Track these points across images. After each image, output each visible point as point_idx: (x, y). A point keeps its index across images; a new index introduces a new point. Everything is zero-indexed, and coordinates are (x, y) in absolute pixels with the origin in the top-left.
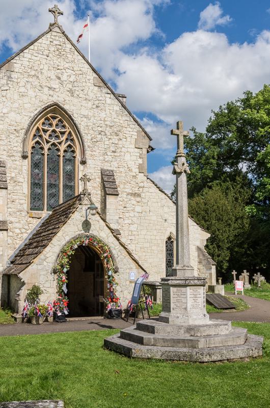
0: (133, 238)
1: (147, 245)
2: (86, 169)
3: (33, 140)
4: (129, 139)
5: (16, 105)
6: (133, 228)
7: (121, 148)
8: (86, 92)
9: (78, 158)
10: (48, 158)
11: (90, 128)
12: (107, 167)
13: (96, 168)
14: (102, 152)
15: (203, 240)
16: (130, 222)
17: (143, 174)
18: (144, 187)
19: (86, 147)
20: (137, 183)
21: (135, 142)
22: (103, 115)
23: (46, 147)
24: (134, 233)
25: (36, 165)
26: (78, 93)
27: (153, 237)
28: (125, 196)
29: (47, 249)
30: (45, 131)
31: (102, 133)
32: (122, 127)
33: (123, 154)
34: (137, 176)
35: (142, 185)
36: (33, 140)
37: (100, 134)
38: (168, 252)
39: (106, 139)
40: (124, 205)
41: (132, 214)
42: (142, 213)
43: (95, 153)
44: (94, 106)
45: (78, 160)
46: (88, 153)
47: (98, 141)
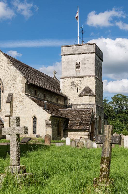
1: (24, 120)
8: (4, 67)
11: (5, 79)
12: (11, 92)
15: (48, 117)
22: (10, 74)
31: (10, 80)
32: (16, 77)
35: (23, 97)
38: (34, 122)
42: (23, 108)
43: (7, 88)
44: (7, 71)
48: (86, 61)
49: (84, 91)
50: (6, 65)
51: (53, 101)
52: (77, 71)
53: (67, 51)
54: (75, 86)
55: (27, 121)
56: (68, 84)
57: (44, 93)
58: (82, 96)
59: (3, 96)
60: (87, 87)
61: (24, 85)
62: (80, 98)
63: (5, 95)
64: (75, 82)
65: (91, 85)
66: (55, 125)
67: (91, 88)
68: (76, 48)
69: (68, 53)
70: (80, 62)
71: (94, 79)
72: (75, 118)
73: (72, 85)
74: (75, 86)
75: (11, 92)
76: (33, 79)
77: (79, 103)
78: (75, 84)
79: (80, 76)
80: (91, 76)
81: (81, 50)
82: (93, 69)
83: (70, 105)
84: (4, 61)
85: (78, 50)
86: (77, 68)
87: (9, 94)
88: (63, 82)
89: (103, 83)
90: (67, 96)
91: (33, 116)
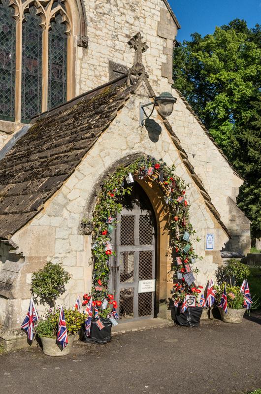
4: (148, 20)
9: (74, 37)
10: (23, 28)
13: (102, 60)
14: (110, 33)
17: (166, 80)
19: (88, 19)
21: (158, 27)
29: (71, 182)
34: (159, 82)
45: (74, 39)
46: (90, 29)
63: (95, 62)
75: (120, 56)
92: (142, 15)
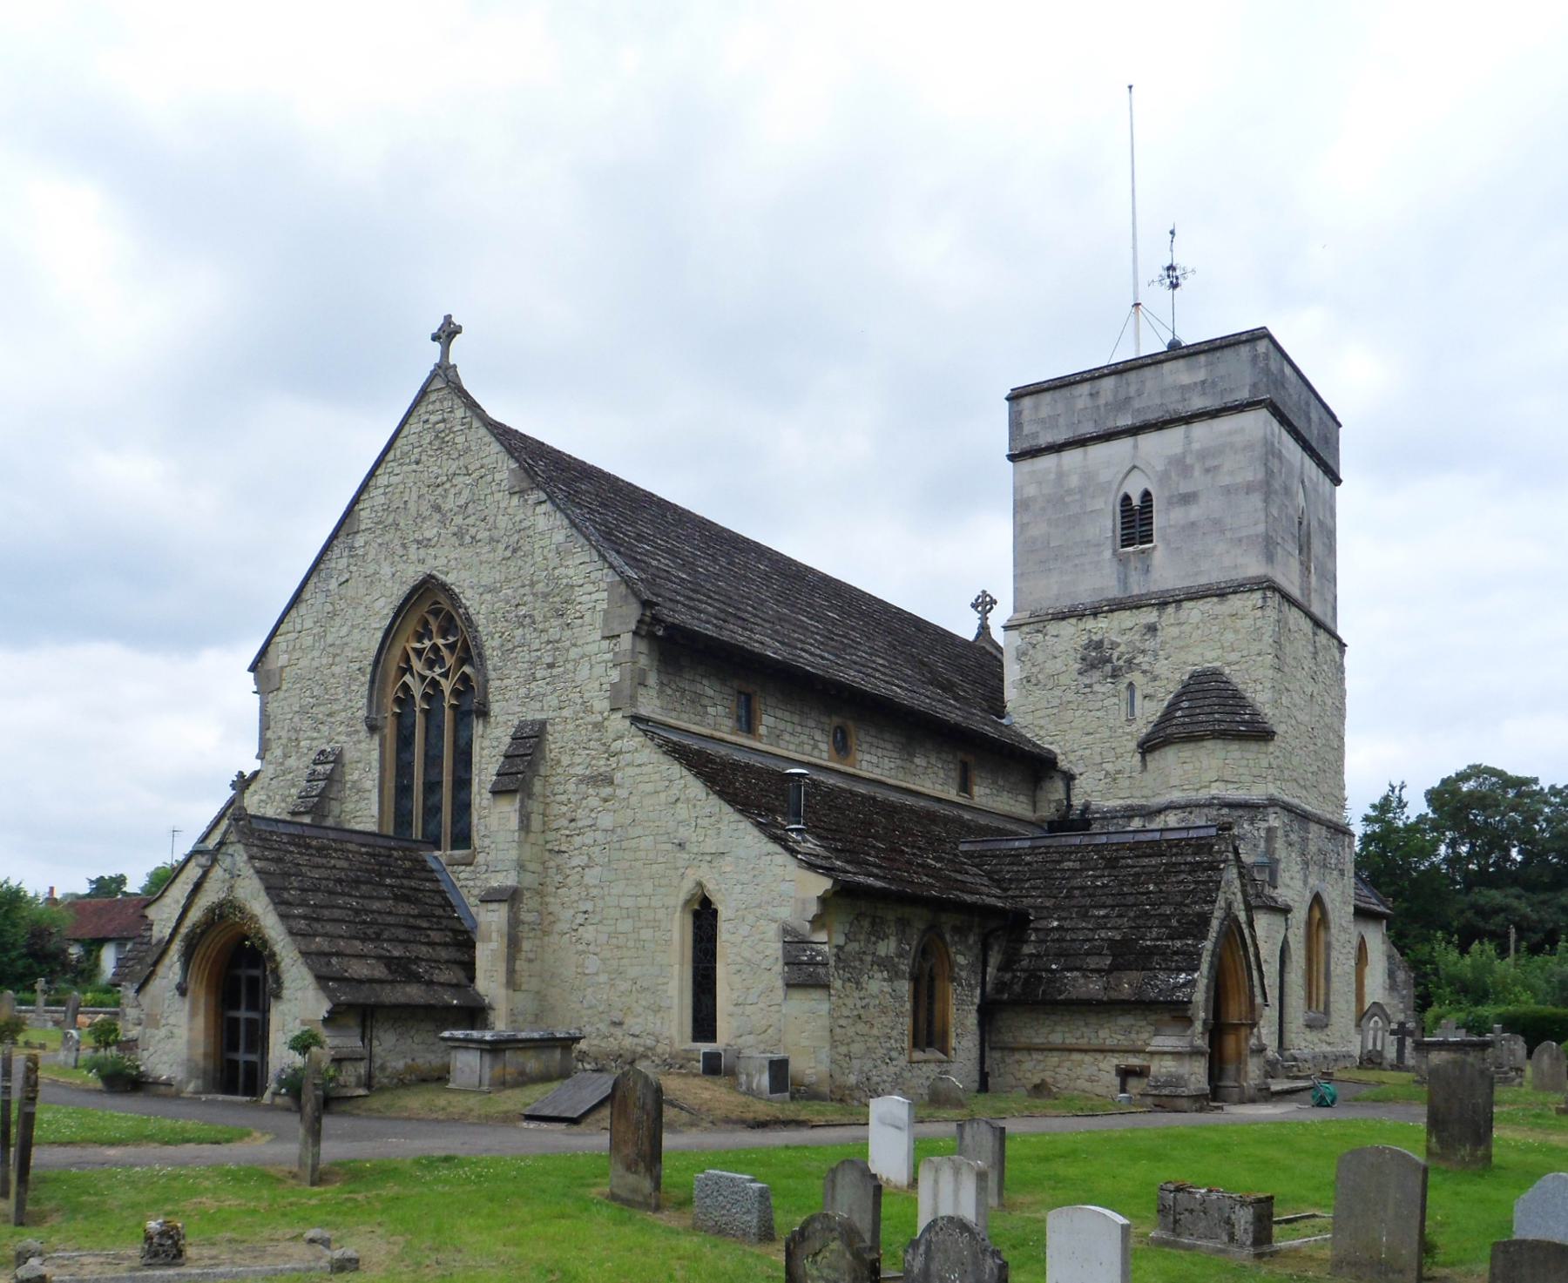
0: (589, 906)
1: (624, 926)
2: (488, 731)
3: (395, 684)
5: (361, 610)
6: (591, 876)
7: (568, 650)
8: (491, 520)
11: (499, 615)
15: (804, 902)
16: (583, 860)
18: (621, 752)
20: (604, 744)
23: (417, 689)
24: (594, 892)
25: (404, 741)
26: (473, 531)
27: (643, 902)
28: (571, 787)
30: (419, 652)
32: (572, 586)
33: (570, 666)
36: (395, 684)
37: (522, 625)
39: (535, 635)
40: (568, 815)
41: (588, 838)
42: (612, 831)
44: (508, 553)
47: (515, 647)
48: (1197, 473)
49: (1185, 704)
50: (503, 505)
51: (929, 784)
52: (1123, 561)
53: (1052, 421)
54: (1115, 674)
55: (646, 934)
56: (1059, 665)
57: (836, 720)
58: (1167, 742)
59: (486, 743)
60: (1204, 673)
61: (626, 640)
62: (1149, 758)
64: (1114, 646)
65: (1234, 657)
66: (884, 964)
67: (1237, 677)
68: (1116, 391)
69: (1061, 436)
70: (1147, 495)
71: (1260, 603)
72: (1084, 916)
73: (1093, 666)
74: (1115, 674)
75: (538, 705)
76: (746, 615)
77: (1143, 802)
78: (1109, 660)
79: (1149, 596)
80: (1238, 588)
81: (1158, 401)
82: (1251, 531)
83: (1075, 813)
84: (489, 478)
85: (1137, 404)
86: (1127, 541)
87: (522, 725)
88: (1024, 654)
89: (1342, 646)
90: (1050, 751)
91: (687, 887)
92: (578, 614)
